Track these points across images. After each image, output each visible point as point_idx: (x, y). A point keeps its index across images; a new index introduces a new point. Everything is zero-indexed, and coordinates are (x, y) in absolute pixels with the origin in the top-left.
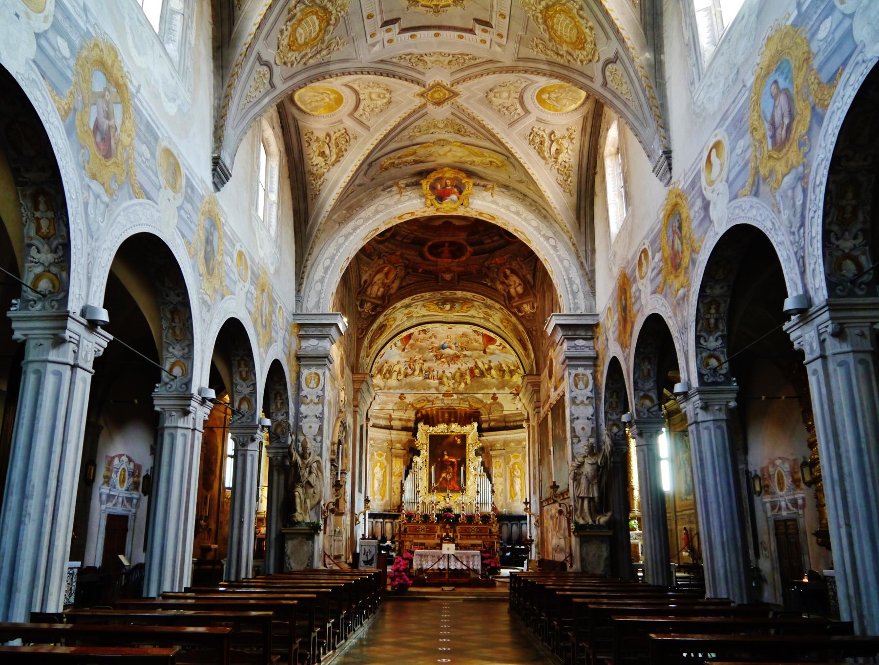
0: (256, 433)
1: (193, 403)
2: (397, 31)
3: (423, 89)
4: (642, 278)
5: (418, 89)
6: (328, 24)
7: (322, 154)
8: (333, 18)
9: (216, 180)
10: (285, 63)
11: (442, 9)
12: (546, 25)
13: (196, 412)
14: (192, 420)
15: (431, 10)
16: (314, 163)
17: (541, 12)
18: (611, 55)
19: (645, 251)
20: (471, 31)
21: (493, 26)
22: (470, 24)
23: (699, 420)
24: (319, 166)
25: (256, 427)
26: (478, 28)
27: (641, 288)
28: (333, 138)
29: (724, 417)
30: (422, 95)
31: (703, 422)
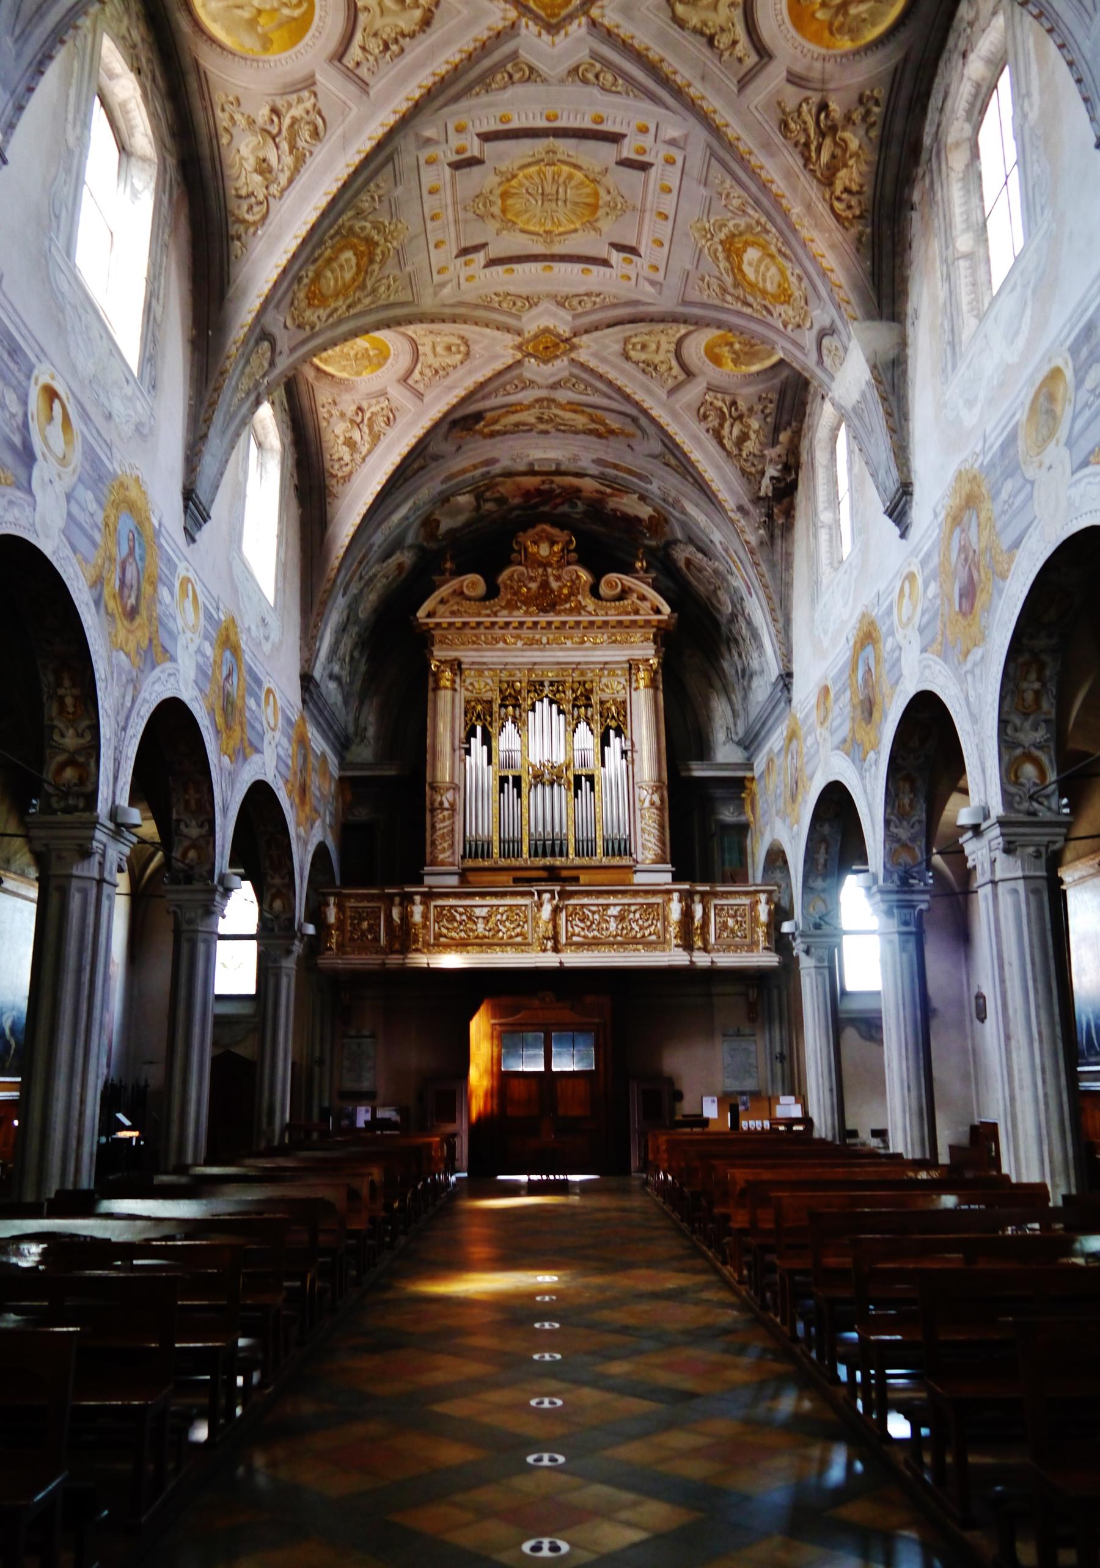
0: (293, 944)
1: (99, 835)
2: (483, 262)
3: (518, 340)
4: (904, 626)
5: (511, 339)
6: (371, 261)
7: (350, 443)
8: (378, 251)
9: (190, 522)
10: (300, 327)
11: (557, 239)
12: (730, 263)
13: (104, 851)
14: (96, 865)
15: (542, 240)
16: (335, 457)
17: (721, 242)
18: (827, 323)
19: (911, 577)
20: (605, 263)
21: (642, 254)
22: (603, 251)
23: (997, 879)
24: (342, 462)
25: (294, 937)
26: (615, 257)
27: (903, 643)
28: (368, 415)
29: (1044, 874)
30: (519, 347)
31: (1002, 880)
